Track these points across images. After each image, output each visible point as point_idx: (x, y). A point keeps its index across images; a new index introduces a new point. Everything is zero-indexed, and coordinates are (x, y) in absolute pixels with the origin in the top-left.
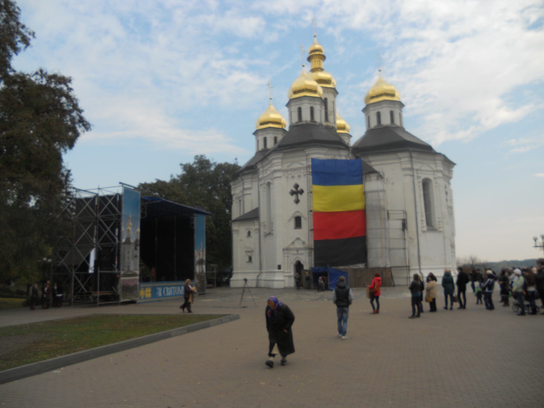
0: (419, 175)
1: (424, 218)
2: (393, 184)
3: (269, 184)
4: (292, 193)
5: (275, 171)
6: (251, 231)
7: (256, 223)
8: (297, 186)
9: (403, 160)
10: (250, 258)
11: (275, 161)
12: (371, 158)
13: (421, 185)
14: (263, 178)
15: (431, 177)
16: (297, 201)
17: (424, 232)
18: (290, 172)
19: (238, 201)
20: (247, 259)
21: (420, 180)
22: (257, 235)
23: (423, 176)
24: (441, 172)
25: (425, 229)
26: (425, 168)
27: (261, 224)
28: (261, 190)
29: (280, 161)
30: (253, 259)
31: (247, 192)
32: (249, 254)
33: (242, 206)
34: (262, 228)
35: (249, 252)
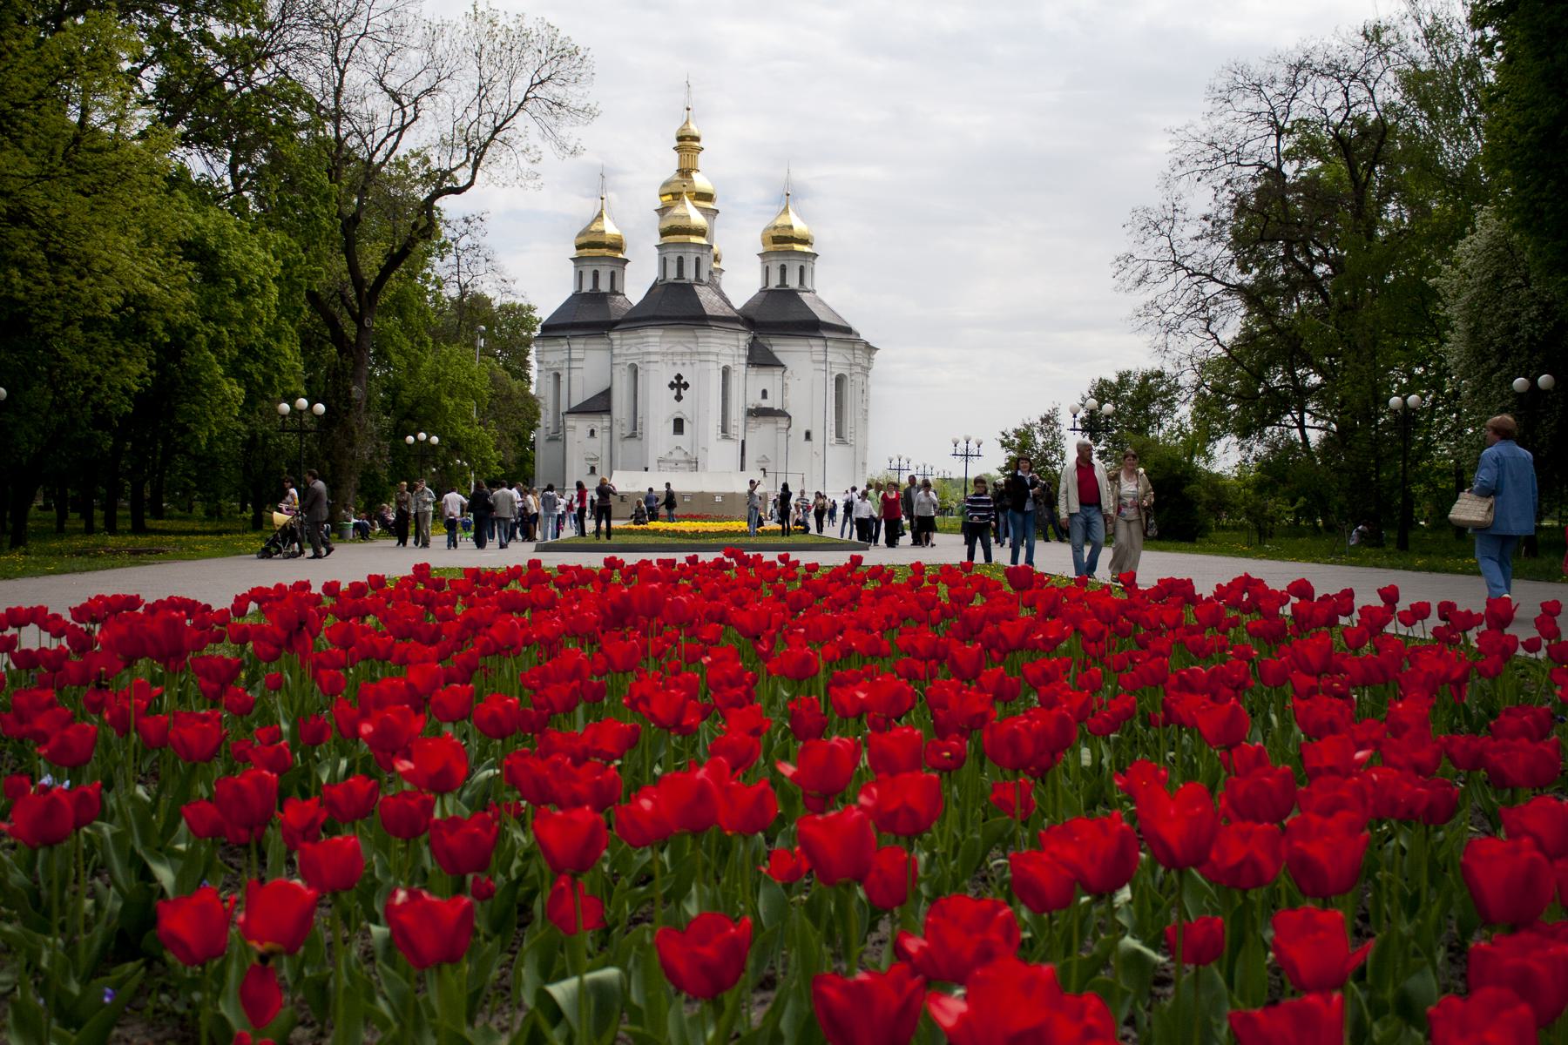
3: (634, 370)
4: (672, 386)
5: (649, 353)
7: (606, 418)
8: (679, 377)
9: (814, 349)
11: (651, 340)
12: (773, 341)
14: (620, 355)
16: (679, 398)
17: (831, 445)
18: (670, 357)
21: (834, 377)
22: (606, 436)
23: (837, 372)
24: (859, 364)
25: (834, 442)
26: (841, 359)
28: (616, 370)
29: (657, 339)
31: (574, 365)
32: (592, 463)
34: (616, 429)
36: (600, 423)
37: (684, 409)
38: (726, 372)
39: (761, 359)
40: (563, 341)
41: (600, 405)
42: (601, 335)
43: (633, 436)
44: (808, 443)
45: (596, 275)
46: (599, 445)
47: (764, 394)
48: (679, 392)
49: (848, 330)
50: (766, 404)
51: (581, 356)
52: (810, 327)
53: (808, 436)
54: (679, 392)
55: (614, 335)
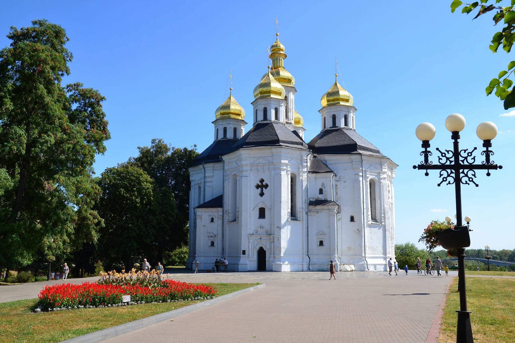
0: (368, 176)
1: (370, 213)
2: (345, 182)
4: (258, 187)
6: (214, 217)
7: (220, 209)
8: (262, 181)
10: (213, 244)
13: (368, 183)
16: (262, 194)
19: (197, 187)
20: (210, 244)
21: (368, 180)
22: (220, 222)
23: (370, 177)
27: (225, 211)
30: (215, 244)
31: (208, 180)
32: (212, 239)
33: (202, 193)
35: (211, 236)
36: (216, 212)
37: (265, 202)
40: (201, 166)
43: (235, 220)
44: (352, 223)
45: (225, 130)
46: (216, 228)
47: (321, 191)
49: (378, 152)
50: (321, 197)
51: (211, 174)
54: (262, 190)
55: (225, 158)
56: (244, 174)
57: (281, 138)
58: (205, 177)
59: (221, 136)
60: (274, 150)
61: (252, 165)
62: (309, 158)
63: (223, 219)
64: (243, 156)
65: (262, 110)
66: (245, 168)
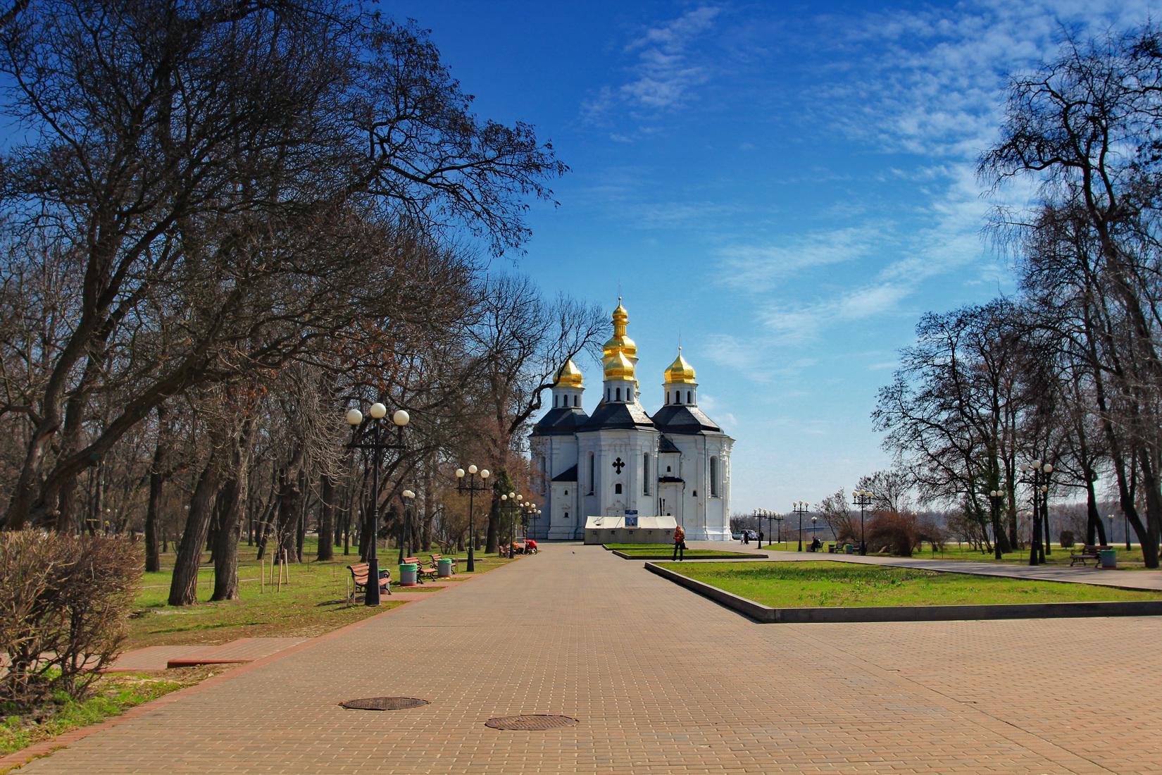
4: (614, 465)
7: (574, 483)
8: (619, 460)
10: (566, 515)
15: (717, 455)
16: (619, 472)
22: (574, 495)
23: (711, 455)
31: (555, 452)
32: (566, 511)
38: (646, 457)
39: (667, 447)
41: (570, 475)
42: (572, 434)
43: (591, 494)
46: (570, 501)
47: (669, 469)
48: (619, 468)
50: (670, 475)
51: (558, 447)
52: (695, 428)
53: (695, 494)
54: (619, 468)
55: (578, 434)
56: (603, 453)
57: (636, 421)
58: (552, 449)
59: (561, 405)
60: (632, 433)
61: (610, 445)
62: (656, 435)
63: (578, 492)
64: (602, 437)
65: (615, 390)
66: (603, 448)
